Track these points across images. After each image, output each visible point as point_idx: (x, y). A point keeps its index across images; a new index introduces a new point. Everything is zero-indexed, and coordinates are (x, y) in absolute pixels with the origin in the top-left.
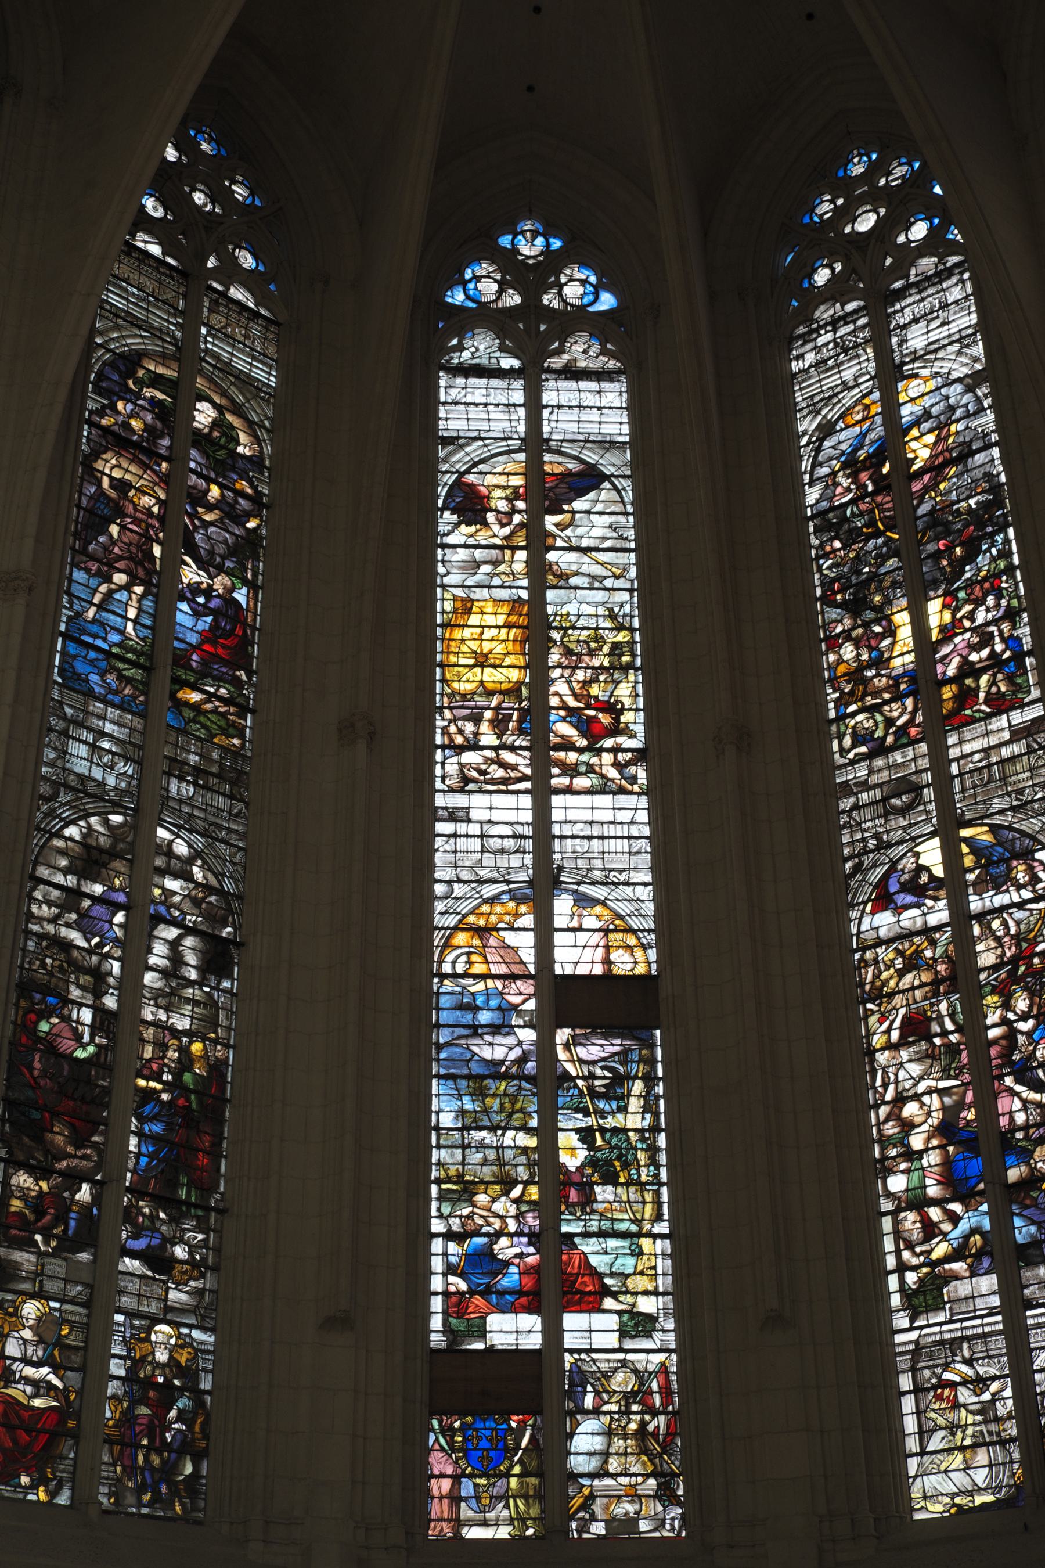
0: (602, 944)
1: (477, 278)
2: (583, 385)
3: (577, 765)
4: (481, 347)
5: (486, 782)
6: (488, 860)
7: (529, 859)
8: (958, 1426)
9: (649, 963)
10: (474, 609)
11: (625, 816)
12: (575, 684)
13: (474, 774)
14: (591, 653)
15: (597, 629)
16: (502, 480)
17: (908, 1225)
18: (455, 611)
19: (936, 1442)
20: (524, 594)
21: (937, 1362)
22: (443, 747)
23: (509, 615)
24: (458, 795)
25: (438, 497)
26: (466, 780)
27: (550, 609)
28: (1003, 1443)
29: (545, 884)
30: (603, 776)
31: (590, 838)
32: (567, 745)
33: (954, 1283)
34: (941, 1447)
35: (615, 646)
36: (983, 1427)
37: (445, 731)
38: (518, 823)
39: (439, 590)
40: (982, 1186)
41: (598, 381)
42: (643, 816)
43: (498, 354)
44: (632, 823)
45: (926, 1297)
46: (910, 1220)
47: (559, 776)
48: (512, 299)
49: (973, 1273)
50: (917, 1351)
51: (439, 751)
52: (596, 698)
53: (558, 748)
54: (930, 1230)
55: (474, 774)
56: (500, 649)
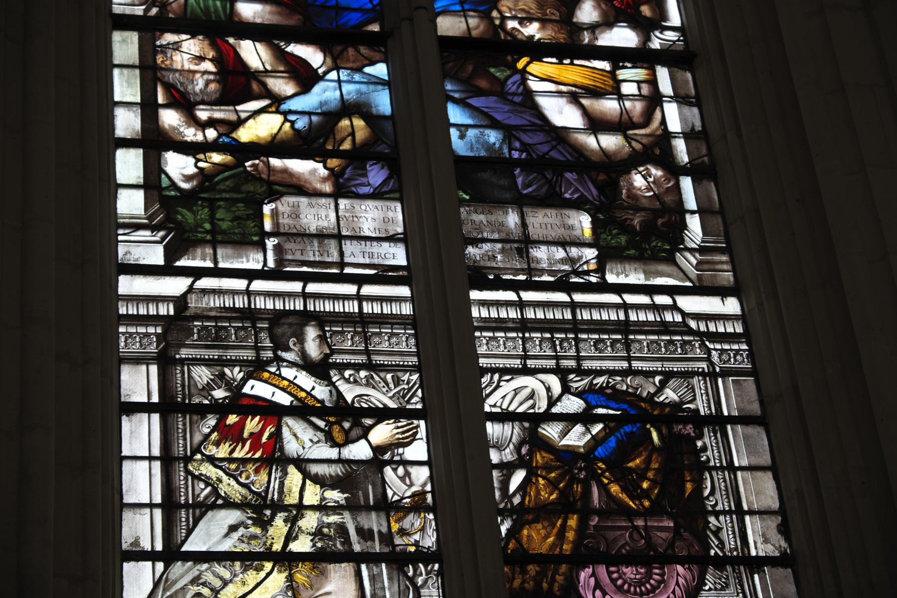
8: (278, 507)
17: (181, 60)
19: (211, 533)
21: (232, 354)
28: (399, 560)
33: (292, 200)
34: (226, 546)
36: (347, 518)
40: (375, 28)
45: (221, 207)
46: (188, 53)
49: (342, 188)
50: (180, 320)
54: (237, 83)
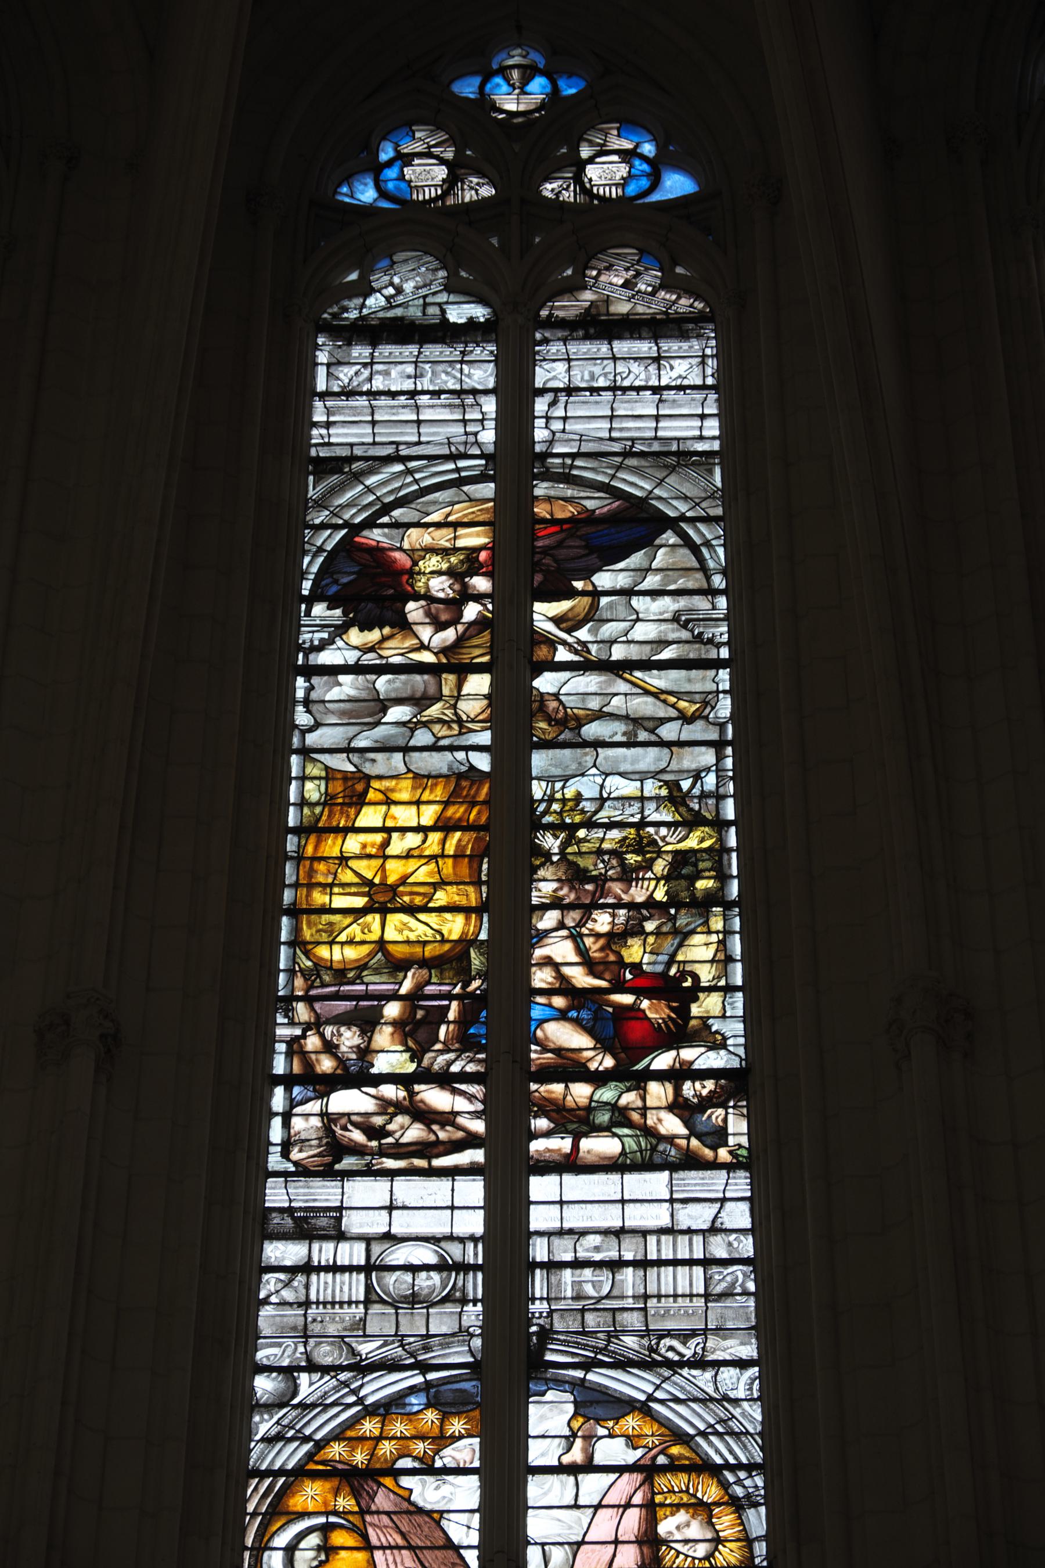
0: (637, 1499)
1: (406, 159)
2: (621, 347)
3: (589, 1109)
4: (405, 285)
5: (382, 1152)
6: (381, 1320)
7: (473, 1315)
9: (748, 1541)
10: (372, 795)
11: (698, 1216)
12: (589, 941)
13: (358, 1136)
14: (628, 876)
15: (642, 824)
16: (442, 538)
18: (328, 801)
20: (482, 762)
22: (288, 1081)
23: (446, 804)
24: (317, 1183)
25: (303, 575)
26: (335, 1148)
27: (538, 790)
29: (509, 1367)
30: (649, 1132)
31: (615, 1265)
32: (568, 1067)
35: (682, 858)
37: (294, 1046)
38: (451, 1238)
39: (294, 759)
41: (656, 338)
42: (739, 1216)
43: (443, 298)
44: (714, 1229)
47: (548, 1134)
48: (477, 190)
51: (279, 1092)
52: (636, 967)
53: (546, 1075)
55: (358, 1136)
56: (424, 873)
